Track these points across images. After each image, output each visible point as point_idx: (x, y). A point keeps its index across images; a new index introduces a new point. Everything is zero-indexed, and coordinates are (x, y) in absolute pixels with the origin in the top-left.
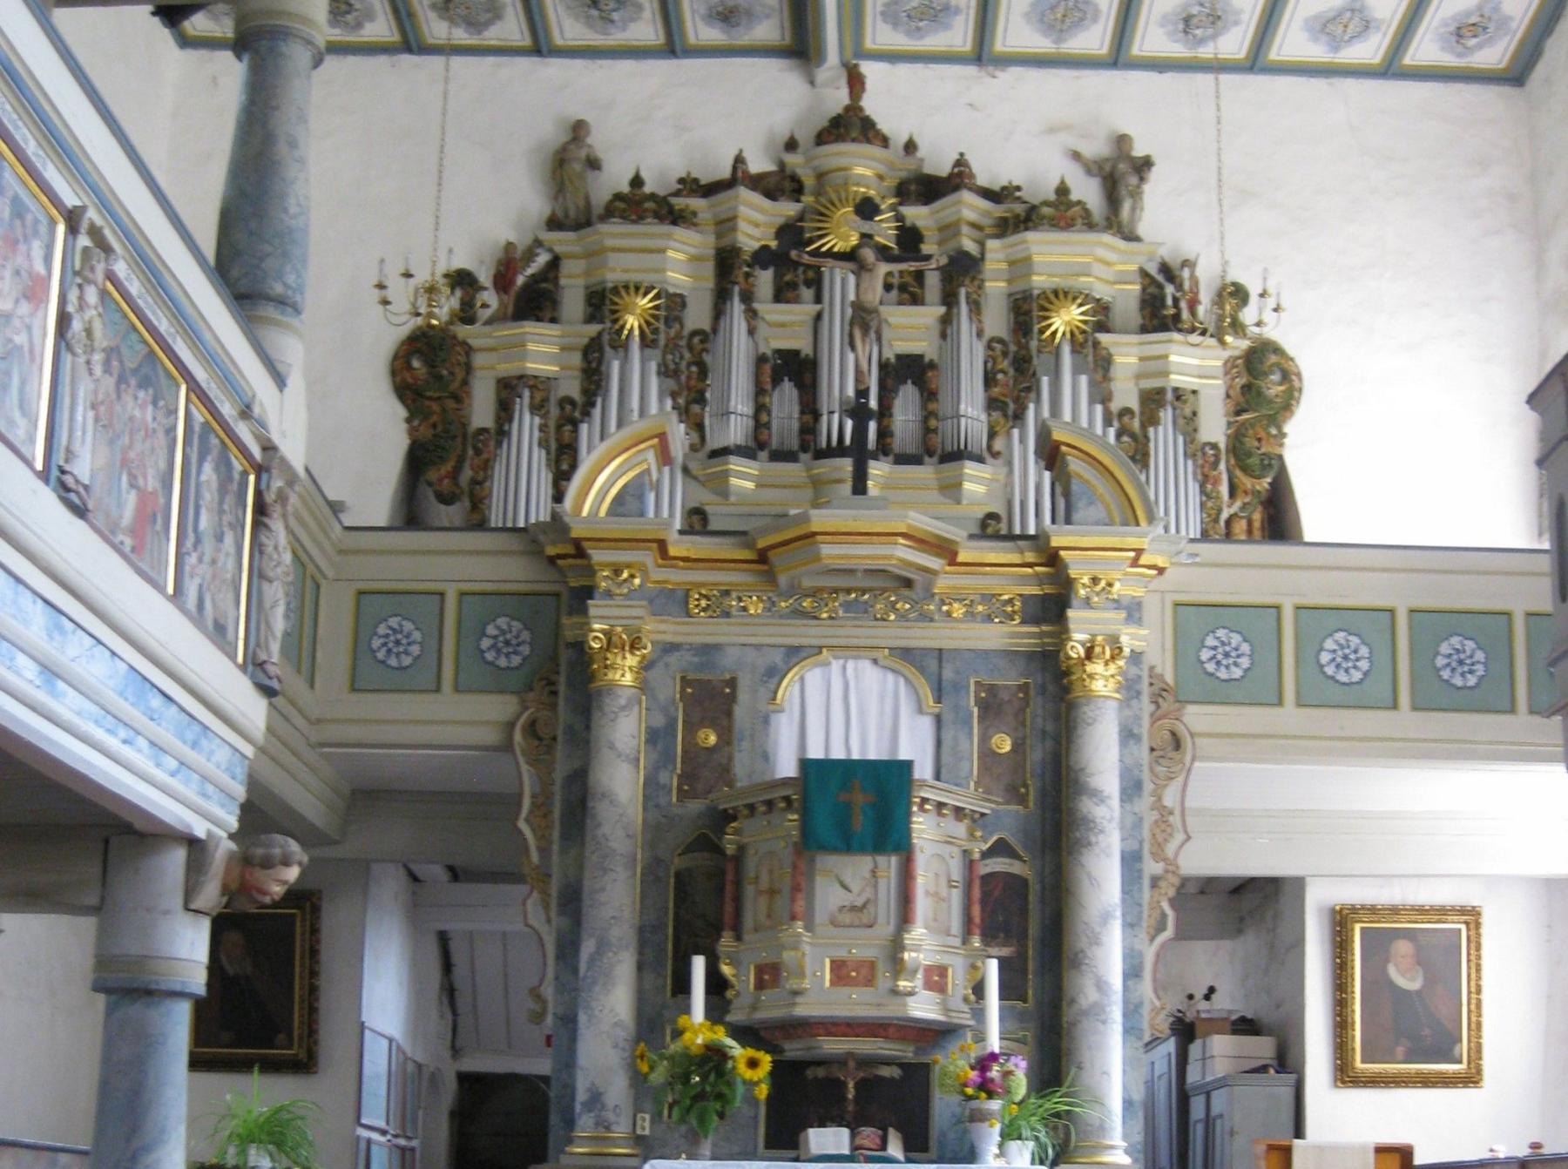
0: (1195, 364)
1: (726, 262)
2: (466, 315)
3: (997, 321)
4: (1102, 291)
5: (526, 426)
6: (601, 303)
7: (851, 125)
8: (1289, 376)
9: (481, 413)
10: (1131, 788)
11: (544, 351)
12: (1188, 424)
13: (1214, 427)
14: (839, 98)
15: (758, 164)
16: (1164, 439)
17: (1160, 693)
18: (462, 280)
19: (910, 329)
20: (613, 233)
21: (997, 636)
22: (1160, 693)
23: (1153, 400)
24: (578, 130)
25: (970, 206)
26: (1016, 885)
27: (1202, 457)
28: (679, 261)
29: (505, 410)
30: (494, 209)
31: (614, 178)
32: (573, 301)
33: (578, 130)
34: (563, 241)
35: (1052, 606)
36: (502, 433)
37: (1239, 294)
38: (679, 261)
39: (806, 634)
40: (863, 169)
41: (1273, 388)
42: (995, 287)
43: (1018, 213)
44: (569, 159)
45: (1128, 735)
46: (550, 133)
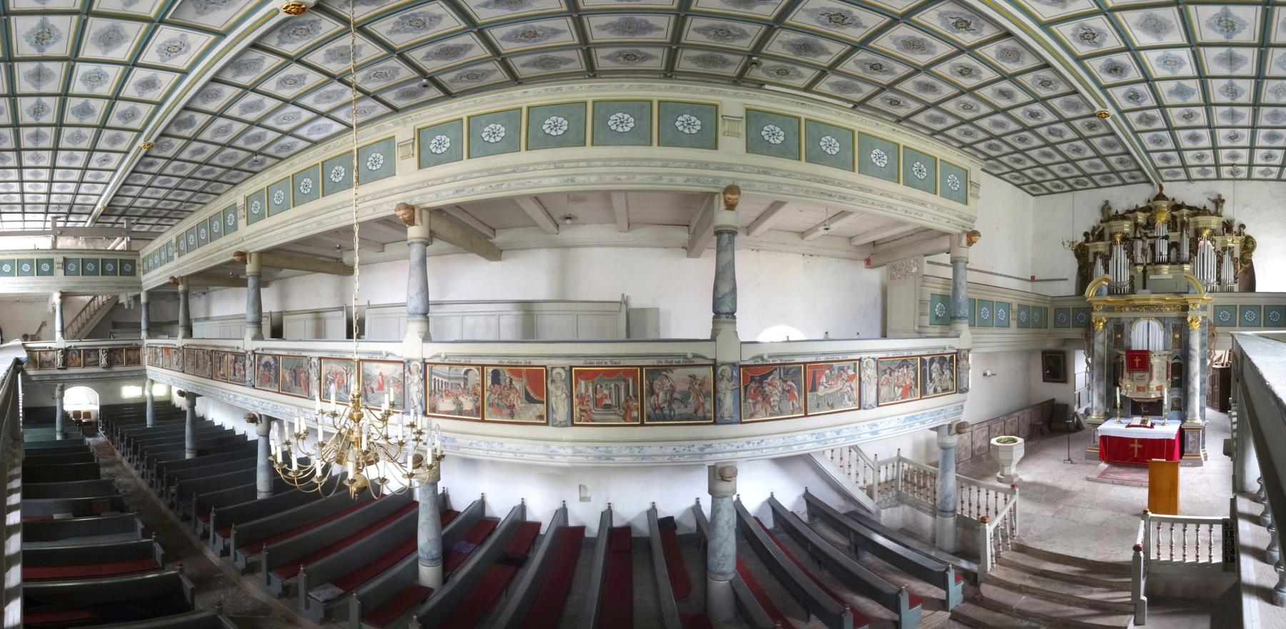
0: (1234, 242)
1: (1136, 225)
2: (1087, 241)
3: (1192, 234)
4: (1214, 226)
5: (1099, 261)
6: (1112, 236)
7: (1161, 197)
8: (1254, 243)
9: (1091, 260)
10: (1203, 345)
11: (1101, 246)
12: (1232, 254)
13: (1237, 254)
14: (1158, 191)
15: (1141, 205)
16: (1227, 258)
17: (1210, 325)
18: (1086, 234)
19: (1174, 236)
20: (1112, 223)
21: (1175, 314)
22: (1210, 325)
23: (1224, 249)
24: (1107, 202)
25: (1185, 211)
26: (1180, 365)
27: (1234, 261)
28: (1127, 227)
29: (1095, 259)
30: (1091, 219)
31: (1113, 212)
32: (1107, 237)
33: (1107, 202)
34: (1104, 225)
35: (1185, 308)
36: (1095, 263)
37: (1243, 226)
38: (1127, 227)
39: (1138, 315)
40: (1164, 204)
41: (1250, 246)
42: (1192, 227)
43: (1197, 211)
44: (1106, 208)
45: (1203, 334)
46: (1101, 203)
